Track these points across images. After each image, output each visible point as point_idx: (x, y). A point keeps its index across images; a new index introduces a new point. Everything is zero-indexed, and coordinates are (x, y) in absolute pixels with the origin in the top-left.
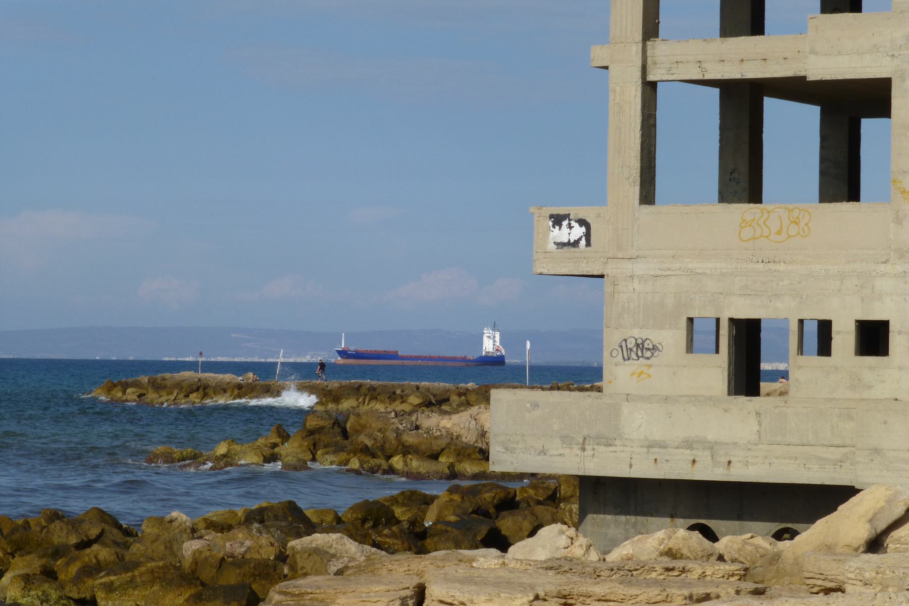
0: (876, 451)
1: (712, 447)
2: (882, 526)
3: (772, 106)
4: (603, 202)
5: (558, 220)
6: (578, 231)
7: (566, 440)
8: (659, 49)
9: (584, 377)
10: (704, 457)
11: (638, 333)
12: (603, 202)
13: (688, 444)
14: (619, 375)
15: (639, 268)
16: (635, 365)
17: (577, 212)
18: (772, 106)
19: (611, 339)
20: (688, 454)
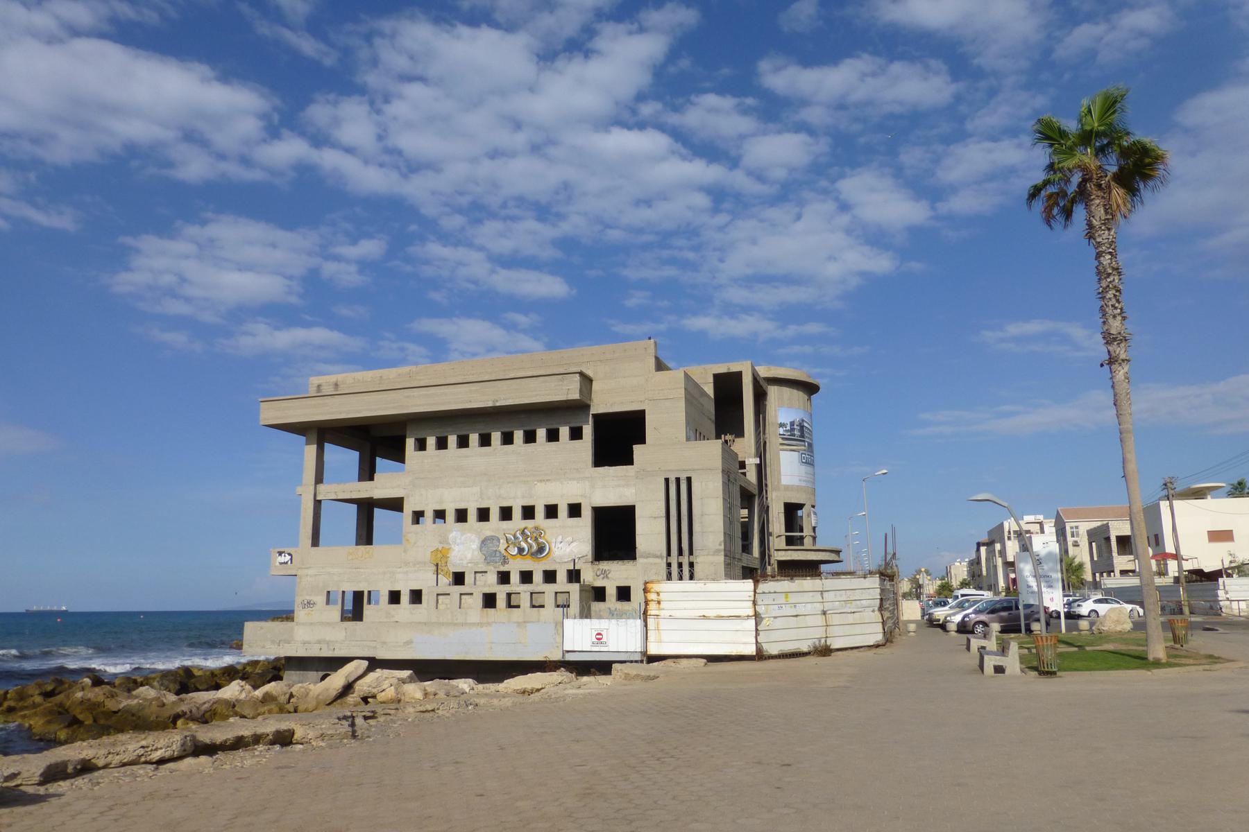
0: (384, 643)
1: (328, 643)
2: (351, 680)
3: (378, 512)
4: (297, 546)
5: (280, 553)
6: (288, 558)
7: (273, 642)
8: (321, 487)
9: (286, 615)
10: (324, 647)
11: (308, 598)
12: (297, 546)
13: (319, 642)
14: (300, 614)
15: (310, 572)
16: (307, 610)
17: (287, 550)
18: (378, 512)
19: (298, 600)
20: (318, 646)
